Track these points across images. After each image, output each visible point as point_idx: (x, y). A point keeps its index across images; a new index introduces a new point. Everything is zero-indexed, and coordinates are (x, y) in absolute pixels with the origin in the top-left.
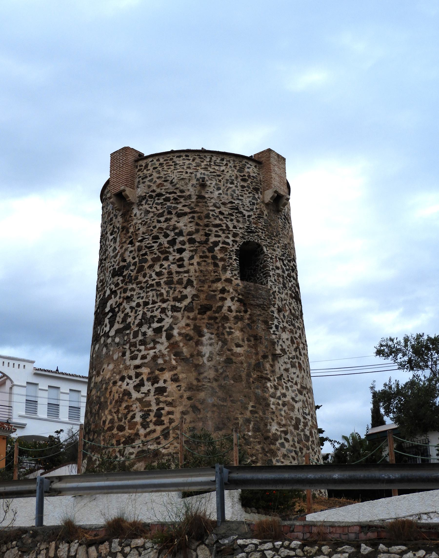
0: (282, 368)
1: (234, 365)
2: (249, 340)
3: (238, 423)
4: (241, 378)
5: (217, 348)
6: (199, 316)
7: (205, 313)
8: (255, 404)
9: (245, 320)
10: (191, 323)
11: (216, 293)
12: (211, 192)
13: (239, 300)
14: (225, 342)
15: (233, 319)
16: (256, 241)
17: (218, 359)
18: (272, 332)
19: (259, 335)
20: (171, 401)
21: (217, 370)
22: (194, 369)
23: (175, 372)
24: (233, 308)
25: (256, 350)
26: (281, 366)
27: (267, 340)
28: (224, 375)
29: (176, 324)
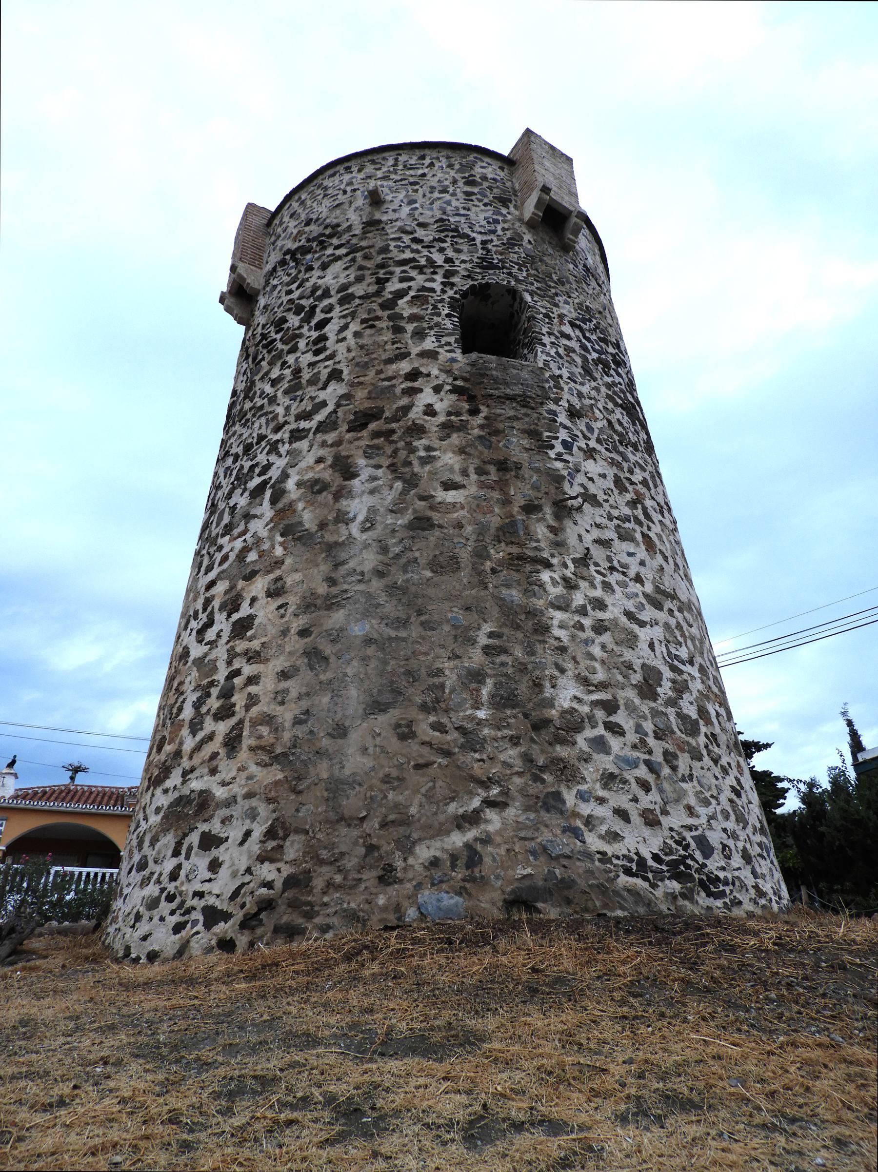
0: (588, 539)
1: (437, 533)
2: (480, 471)
3: (442, 686)
4: (458, 563)
5: (390, 497)
6: (349, 436)
7: (364, 426)
8: (501, 627)
9: (472, 429)
10: (326, 455)
11: (394, 382)
12: (394, 211)
13: (455, 390)
14: (411, 482)
15: (437, 429)
16: (505, 283)
17: (389, 522)
18: (553, 456)
19: (515, 459)
20: (258, 649)
21: (384, 550)
22: (324, 555)
23: (278, 573)
24: (438, 407)
25: (503, 491)
26: (583, 533)
27: (537, 470)
28: (403, 560)
29: (294, 466)
